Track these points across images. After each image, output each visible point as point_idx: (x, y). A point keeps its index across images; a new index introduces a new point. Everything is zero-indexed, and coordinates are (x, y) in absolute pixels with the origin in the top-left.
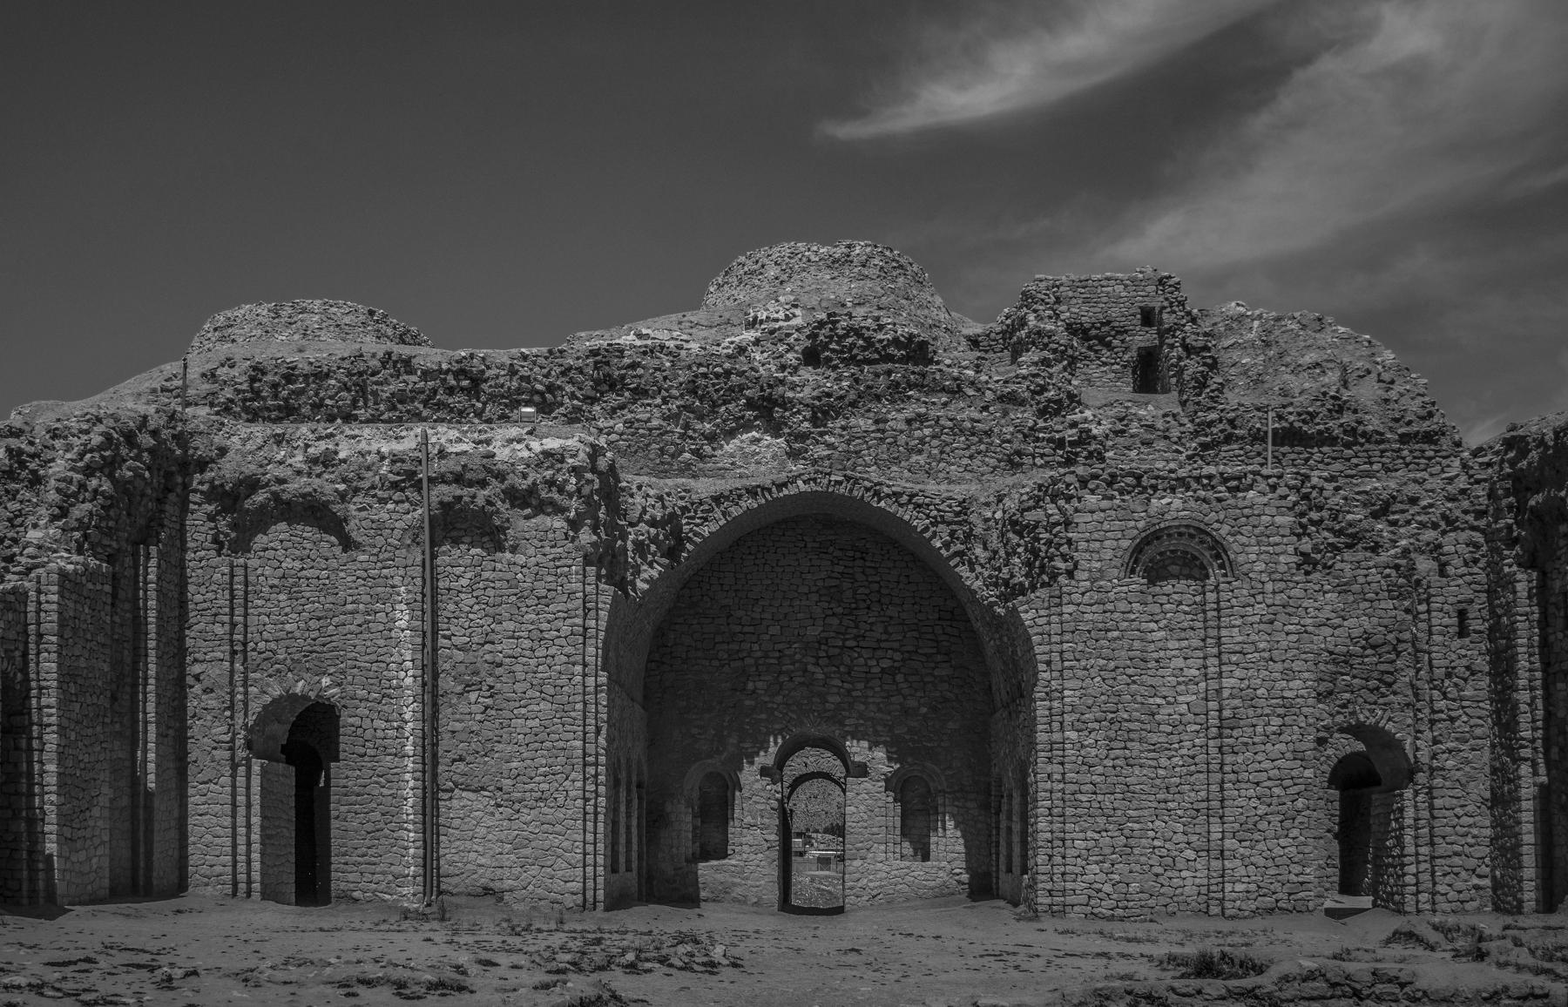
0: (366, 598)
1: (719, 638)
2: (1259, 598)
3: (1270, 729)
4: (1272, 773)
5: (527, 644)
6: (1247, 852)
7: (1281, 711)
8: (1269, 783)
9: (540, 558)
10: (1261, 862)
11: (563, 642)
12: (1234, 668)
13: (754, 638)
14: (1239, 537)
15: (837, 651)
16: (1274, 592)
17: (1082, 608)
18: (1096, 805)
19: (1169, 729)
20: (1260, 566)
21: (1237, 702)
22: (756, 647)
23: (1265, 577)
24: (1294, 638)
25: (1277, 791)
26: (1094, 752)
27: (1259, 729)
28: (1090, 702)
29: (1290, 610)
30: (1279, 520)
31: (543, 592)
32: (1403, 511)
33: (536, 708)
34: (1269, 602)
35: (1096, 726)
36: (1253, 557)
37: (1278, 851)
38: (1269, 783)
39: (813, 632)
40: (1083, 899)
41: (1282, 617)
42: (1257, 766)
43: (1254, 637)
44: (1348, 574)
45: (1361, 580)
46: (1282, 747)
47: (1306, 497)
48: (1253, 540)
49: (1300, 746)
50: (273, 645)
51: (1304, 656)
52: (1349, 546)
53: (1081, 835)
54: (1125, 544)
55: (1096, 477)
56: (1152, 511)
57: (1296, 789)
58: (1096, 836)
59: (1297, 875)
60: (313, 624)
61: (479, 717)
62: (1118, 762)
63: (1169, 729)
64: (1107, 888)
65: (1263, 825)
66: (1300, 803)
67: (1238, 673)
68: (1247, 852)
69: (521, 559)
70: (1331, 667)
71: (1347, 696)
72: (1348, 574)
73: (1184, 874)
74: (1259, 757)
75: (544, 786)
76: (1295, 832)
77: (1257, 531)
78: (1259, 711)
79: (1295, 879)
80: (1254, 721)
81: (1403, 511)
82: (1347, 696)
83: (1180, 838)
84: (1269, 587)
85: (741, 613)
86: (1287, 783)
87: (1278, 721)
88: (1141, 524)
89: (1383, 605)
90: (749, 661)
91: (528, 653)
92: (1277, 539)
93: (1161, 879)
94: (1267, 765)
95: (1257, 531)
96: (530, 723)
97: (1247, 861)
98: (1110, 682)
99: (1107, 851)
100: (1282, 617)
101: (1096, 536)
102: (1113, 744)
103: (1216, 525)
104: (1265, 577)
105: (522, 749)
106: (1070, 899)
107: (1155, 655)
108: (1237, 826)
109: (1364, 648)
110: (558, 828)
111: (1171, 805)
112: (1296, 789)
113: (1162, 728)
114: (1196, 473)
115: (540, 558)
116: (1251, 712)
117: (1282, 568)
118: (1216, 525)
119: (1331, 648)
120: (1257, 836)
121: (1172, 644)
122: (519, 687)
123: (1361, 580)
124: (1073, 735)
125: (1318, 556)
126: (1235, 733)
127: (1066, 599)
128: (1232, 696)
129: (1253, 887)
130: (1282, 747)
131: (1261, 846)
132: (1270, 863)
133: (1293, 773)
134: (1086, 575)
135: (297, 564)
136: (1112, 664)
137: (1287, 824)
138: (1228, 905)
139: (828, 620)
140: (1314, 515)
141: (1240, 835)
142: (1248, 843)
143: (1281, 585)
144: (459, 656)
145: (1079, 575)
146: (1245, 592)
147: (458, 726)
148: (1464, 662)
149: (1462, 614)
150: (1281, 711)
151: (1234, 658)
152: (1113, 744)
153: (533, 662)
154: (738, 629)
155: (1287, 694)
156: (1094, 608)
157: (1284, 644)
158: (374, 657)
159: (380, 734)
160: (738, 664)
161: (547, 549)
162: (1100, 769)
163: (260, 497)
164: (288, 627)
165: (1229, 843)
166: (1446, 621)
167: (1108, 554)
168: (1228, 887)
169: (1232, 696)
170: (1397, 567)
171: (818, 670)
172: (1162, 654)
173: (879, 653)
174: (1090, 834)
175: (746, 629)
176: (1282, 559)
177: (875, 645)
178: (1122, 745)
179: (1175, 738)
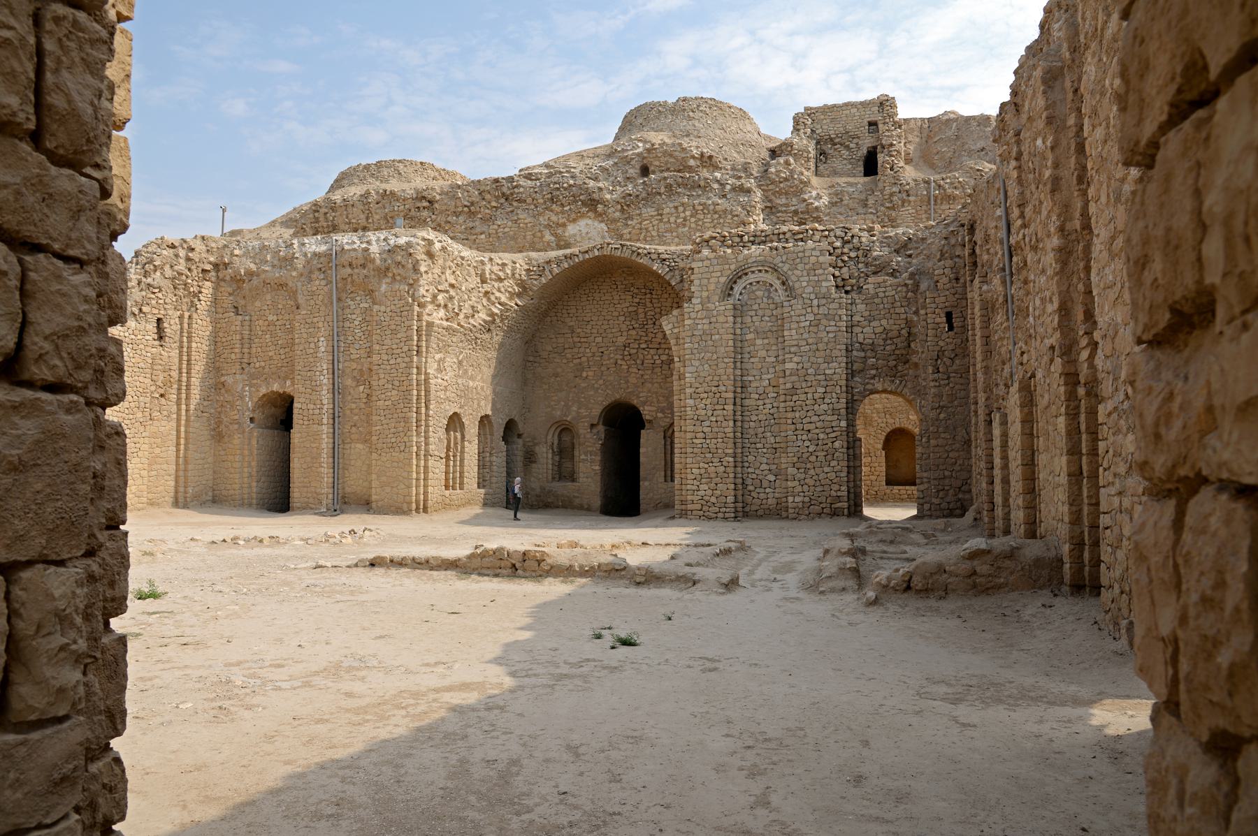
0: (305, 336)
1: (566, 346)
2: (809, 310)
3: (816, 396)
4: (819, 424)
5: (385, 357)
6: (803, 476)
7: (823, 383)
8: (817, 431)
9: (393, 307)
10: (811, 482)
11: (404, 355)
12: (792, 355)
13: (587, 345)
14: (795, 272)
15: (635, 351)
16: (818, 306)
17: (697, 322)
18: (705, 446)
19: (757, 396)
20: (810, 289)
21: (794, 378)
22: (588, 350)
23: (813, 296)
24: (831, 335)
25: (821, 436)
26: (704, 412)
27: (810, 396)
28: (701, 381)
29: (829, 317)
30: (821, 259)
31: (394, 327)
32: (917, 248)
33: (389, 394)
34: (816, 312)
35: (706, 395)
36: (804, 284)
37: (822, 476)
38: (817, 431)
39: (621, 340)
40: (699, 507)
41: (824, 322)
42: (808, 420)
43: (805, 336)
44: (872, 292)
45: (881, 295)
46: (825, 407)
47: (848, 242)
48: (805, 273)
49: (837, 406)
50: (263, 364)
51: (838, 347)
52: (875, 273)
53: (697, 466)
54: (723, 280)
55: (715, 238)
56: (740, 258)
57: (833, 435)
58: (706, 466)
59: (836, 491)
60: (282, 351)
61: (364, 400)
62: (719, 419)
63: (757, 396)
64: (713, 500)
65: (813, 458)
66: (837, 444)
67: (795, 359)
68: (803, 476)
69: (383, 308)
70: (863, 354)
71: (873, 372)
72: (872, 292)
73: (767, 490)
74: (809, 414)
75: (393, 440)
76: (834, 463)
77: (807, 267)
78: (809, 384)
79: (835, 494)
80: (807, 390)
81: (917, 248)
82: (873, 372)
83: (764, 467)
84: (815, 302)
85: (579, 330)
86: (828, 431)
87: (823, 390)
88: (733, 267)
89: (897, 310)
90: (584, 359)
91: (386, 362)
92: (821, 271)
93: (753, 494)
94: (815, 419)
95: (807, 267)
96: (387, 403)
97: (802, 482)
98: (714, 367)
99: (713, 475)
100: (824, 322)
101: (704, 276)
102: (717, 407)
103: (780, 265)
104: (813, 296)
105: (382, 418)
106: (690, 507)
107: (748, 349)
108: (795, 459)
109: (885, 340)
110: (400, 464)
111: (759, 446)
112: (833, 435)
113: (752, 396)
114: (776, 232)
115: (393, 307)
116: (804, 385)
117: (824, 290)
118: (780, 265)
119: (861, 340)
120: (809, 466)
121: (759, 342)
122: (381, 383)
123: (881, 295)
124: (690, 402)
125: (854, 281)
126: (795, 398)
127: (686, 316)
128: (791, 375)
129: (807, 499)
130: (825, 407)
131: (812, 472)
132: (818, 483)
133: (834, 424)
134: (699, 300)
135: (275, 318)
136: (715, 356)
137: (829, 457)
138: (790, 511)
139: (630, 332)
140: (853, 254)
141: (797, 465)
142: (802, 470)
143: (824, 301)
144: (354, 365)
145: (694, 301)
146: (800, 307)
147: (354, 406)
148: (951, 347)
149: (949, 316)
150: (822, 383)
151: (793, 349)
152: (717, 407)
153: (388, 367)
154: (578, 339)
155: (827, 372)
156: (704, 321)
157: (826, 340)
158: (308, 368)
159: (311, 412)
160: (578, 361)
161: (396, 302)
162: (707, 423)
163: (255, 281)
164: (270, 354)
165: (791, 471)
166: (938, 320)
167: (712, 287)
168: (790, 499)
169: (791, 375)
170: (906, 285)
171: (624, 363)
172: (752, 348)
173: (660, 351)
174: (702, 465)
175: (583, 340)
176: (824, 284)
177: (658, 346)
178: (722, 407)
179: (761, 402)
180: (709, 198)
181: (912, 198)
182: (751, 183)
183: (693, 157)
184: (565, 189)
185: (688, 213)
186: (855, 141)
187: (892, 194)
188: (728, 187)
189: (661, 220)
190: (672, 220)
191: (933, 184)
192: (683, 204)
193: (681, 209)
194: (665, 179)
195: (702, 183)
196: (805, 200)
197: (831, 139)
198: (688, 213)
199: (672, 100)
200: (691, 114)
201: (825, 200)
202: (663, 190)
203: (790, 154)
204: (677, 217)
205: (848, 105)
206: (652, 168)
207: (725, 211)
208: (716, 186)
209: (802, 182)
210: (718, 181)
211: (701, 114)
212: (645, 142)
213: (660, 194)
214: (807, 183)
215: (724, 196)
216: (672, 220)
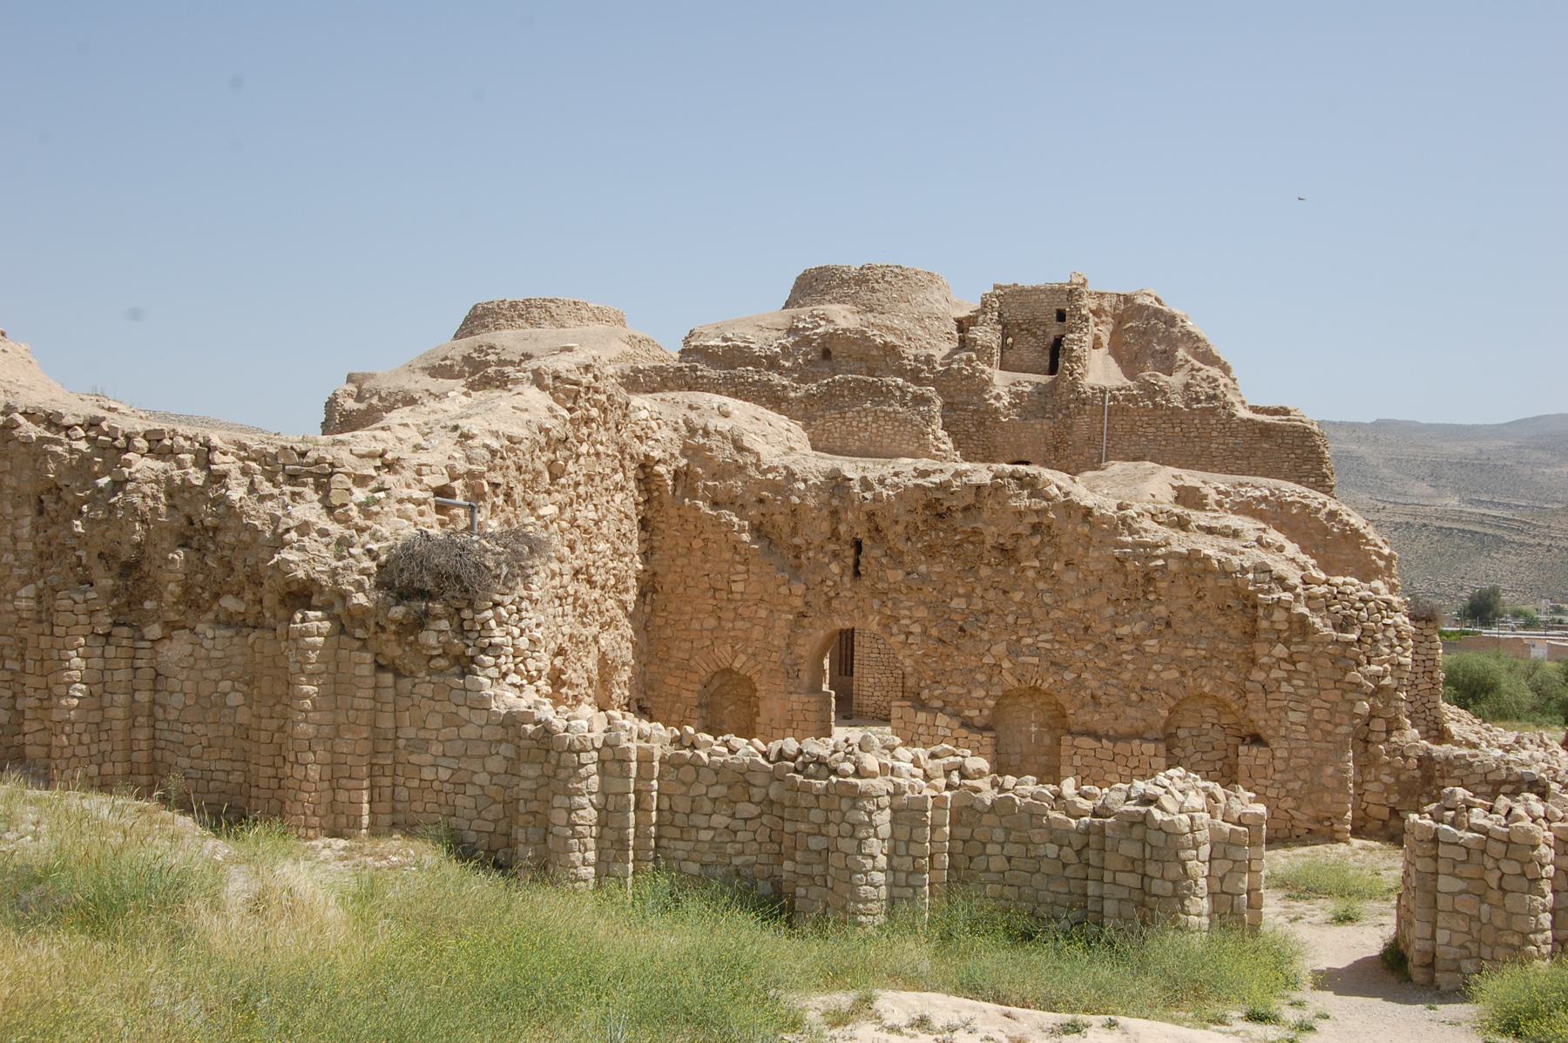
180: (890, 406)
181: (1087, 407)
182: (930, 391)
183: (876, 346)
184: (750, 384)
185: (870, 419)
186: (1043, 328)
187: (1069, 401)
188: (909, 396)
189: (843, 423)
190: (855, 423)
191: (1108, 395)
192: (865, 410)
193: (863, 414)
194: (850, 382)
195: (884, 389)
196: (986, 400)
197: (1019, 325)
198: (870, 419)
199: (855, 265)
200: (876, 285)
201: (1006, 400)
202: (846, 393)
203: (972, 350)
204: (860, 422)
205: (1036, 290)
206: (834, 353)
207: (905, 420)
208: (898, 393)
209: (983, 380)
210: (898, 387)
211: (886, 286)
212: (829, 321)
213: (843, 396)
214: (989, 382)
215: (905, 404)
216: (855, 423)
